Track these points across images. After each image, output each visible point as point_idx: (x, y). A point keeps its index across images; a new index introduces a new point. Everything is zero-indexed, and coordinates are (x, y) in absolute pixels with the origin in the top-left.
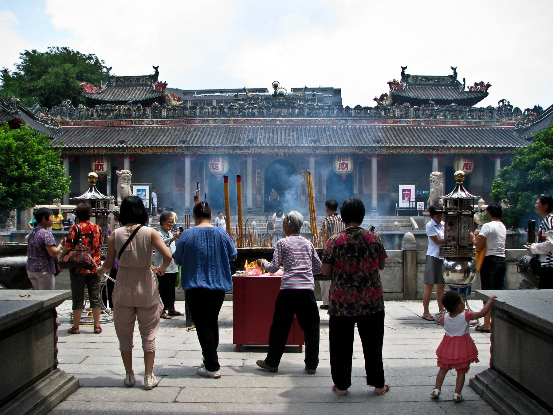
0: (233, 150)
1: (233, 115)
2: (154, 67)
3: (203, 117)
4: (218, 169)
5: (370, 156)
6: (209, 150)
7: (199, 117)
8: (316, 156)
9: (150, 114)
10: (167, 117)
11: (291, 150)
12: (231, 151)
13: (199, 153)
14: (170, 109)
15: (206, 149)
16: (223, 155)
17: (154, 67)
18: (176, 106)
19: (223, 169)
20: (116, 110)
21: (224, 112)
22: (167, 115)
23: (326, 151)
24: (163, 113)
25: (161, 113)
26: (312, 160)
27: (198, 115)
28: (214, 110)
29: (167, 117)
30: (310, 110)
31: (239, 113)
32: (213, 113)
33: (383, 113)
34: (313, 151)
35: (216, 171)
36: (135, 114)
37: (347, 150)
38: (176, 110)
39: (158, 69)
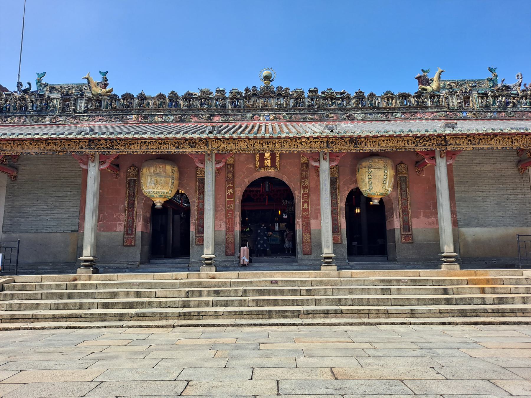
0: (177, 148)
2: (101, 72)
5: (432, 155)
6: (132, 147)
8: (333, 156)
10: (85, 111)
11: (286, 146)
14: (90, 100)
17: (101, 72)
18: (100, 95)
21: (177, 105)
22: (85, 107)
23: (352, 147)
26: (325, 166)
27: (135, 107)
30: (312, 100)
31: (202, 104)
33: (429, 103)
34: (328, 146)
37: (391, 144)
39: (108, 76)
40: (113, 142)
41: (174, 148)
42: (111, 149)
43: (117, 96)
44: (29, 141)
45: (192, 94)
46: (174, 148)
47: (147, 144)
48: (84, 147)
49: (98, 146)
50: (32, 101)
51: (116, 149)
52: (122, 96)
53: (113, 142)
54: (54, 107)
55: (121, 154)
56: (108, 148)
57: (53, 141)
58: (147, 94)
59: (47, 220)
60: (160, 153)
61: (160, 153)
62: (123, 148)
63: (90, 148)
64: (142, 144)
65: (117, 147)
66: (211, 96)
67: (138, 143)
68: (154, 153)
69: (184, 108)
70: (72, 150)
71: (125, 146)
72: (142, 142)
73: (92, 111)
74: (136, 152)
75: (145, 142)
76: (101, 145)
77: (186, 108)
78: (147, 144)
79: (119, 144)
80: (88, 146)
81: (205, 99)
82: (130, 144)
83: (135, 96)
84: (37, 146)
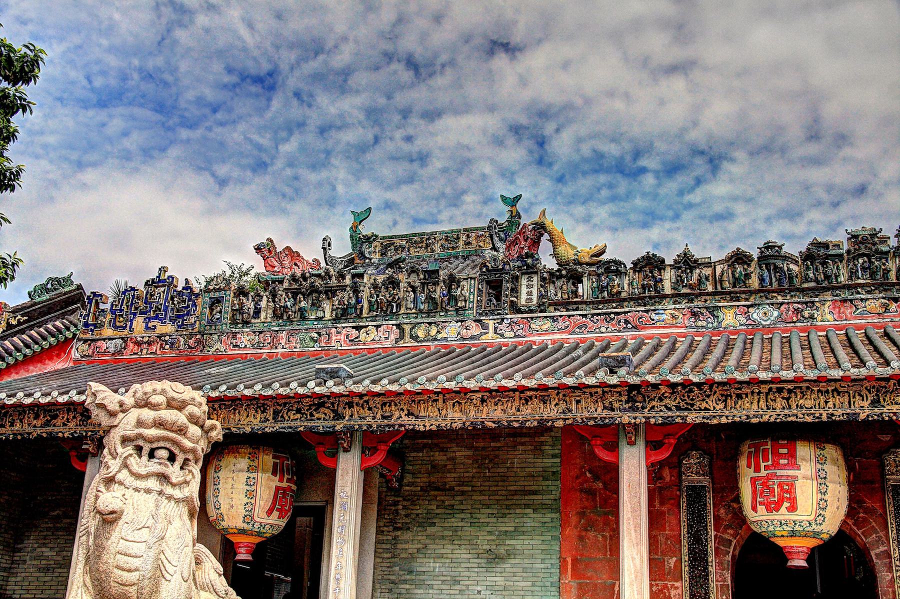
0: (875, 403)
1: (826, 285)
3: (690, 298)
4: (793, 508)
7: (676, 297)
9: (474, 298)
10: (541, 307)
12: (863, 409)
13: (693, 418)
14: (553, 276)
15: (725, 398)
16: (819, 433)
19: (822, 506)
20: (343, 288)
22: (541, 296)
24: (524, 290)
25: (515, 291)
27: (668, 290)
28: (739, 269)
29: (541, 307)
32: (736, 281)
35: (783, 513)
36: (415, 300)
38: (577, 278)
40: (691, 391)
41: (866, 404)
42: (686, 409)
43: (618, 263)
44: (479, 395)
45: (826, 246)
46: (866, 404)
47: (786, 395)
48: (616, 405)
49: (654, 403)
50: (414, 289)
51: (701, 409)
52: (635, 264)
53: (691, 391)
54: (466, 301)
55: (715, 422)
56: (678, 408)
57: (539, 393)
58: (698, 253)
59: (479, 592)
60: (824, 418)
61: (824, 418)
62: (721, 406)
63: (633, 409)
64: (771, 396)
65: (704, 405)
66: (884, 248)
67: (759, 393)
68: (809, 419)
69: (805, 285)
70: (586, 414)
71: (725, 401)
72: (770, 389)
73: (557, 305)
74: (755, 416)
75: (780, 390)
76: (661, 400)
77: (812, 284)
78: (786, 395)
79: (708, 396)
80: (627, 402)
81: (868, 256)
82: (739, 396)
83: (669, 261)
84: (500, 407)
